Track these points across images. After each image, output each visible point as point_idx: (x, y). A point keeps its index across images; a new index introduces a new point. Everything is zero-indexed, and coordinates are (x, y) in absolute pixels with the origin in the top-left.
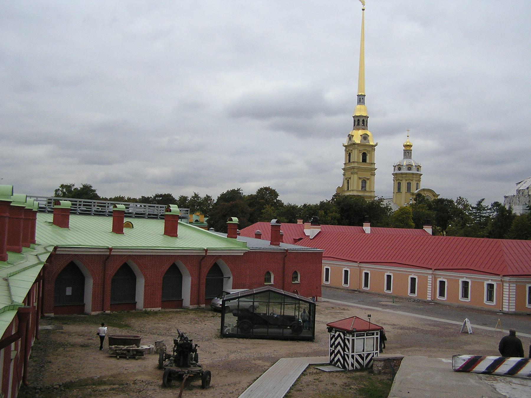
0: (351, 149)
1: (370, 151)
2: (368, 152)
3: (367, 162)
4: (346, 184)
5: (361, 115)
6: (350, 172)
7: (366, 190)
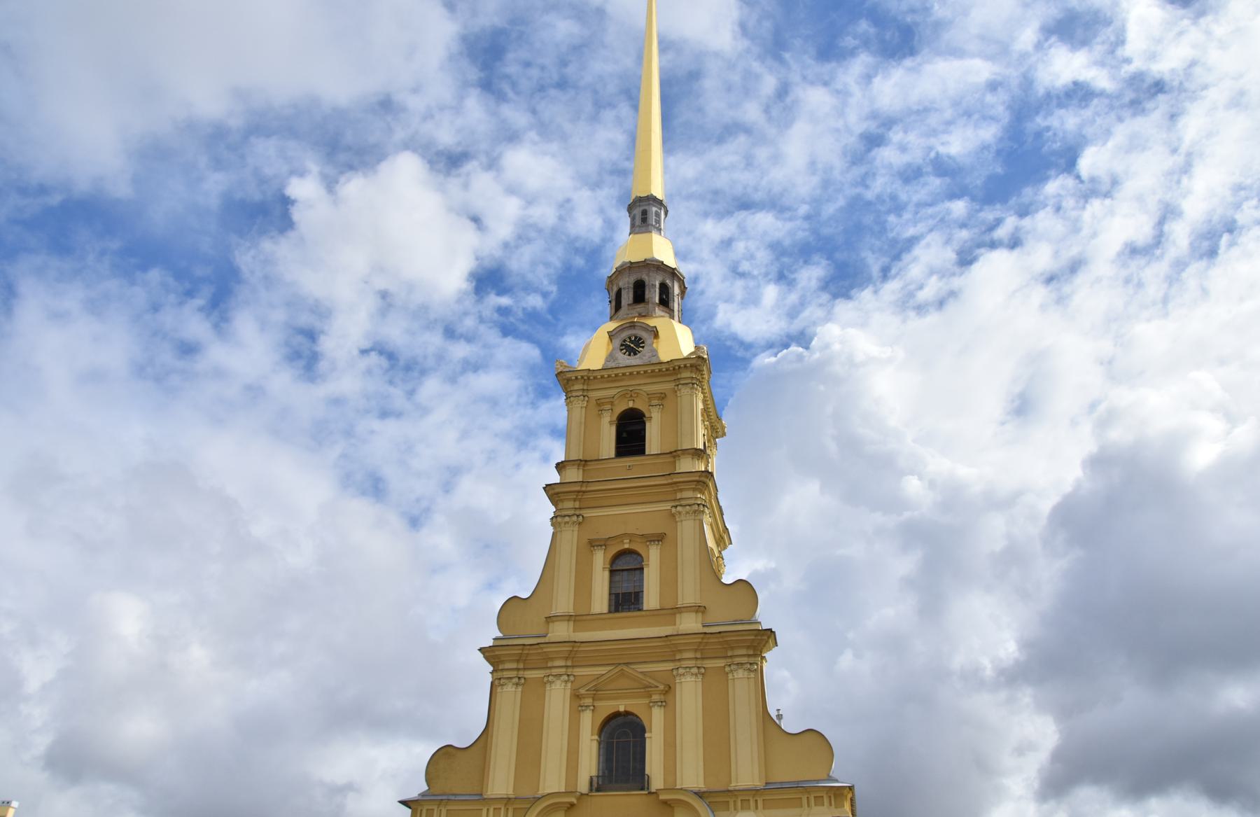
1: (662, 396)
2: (655, 402)
7: (640, 610)
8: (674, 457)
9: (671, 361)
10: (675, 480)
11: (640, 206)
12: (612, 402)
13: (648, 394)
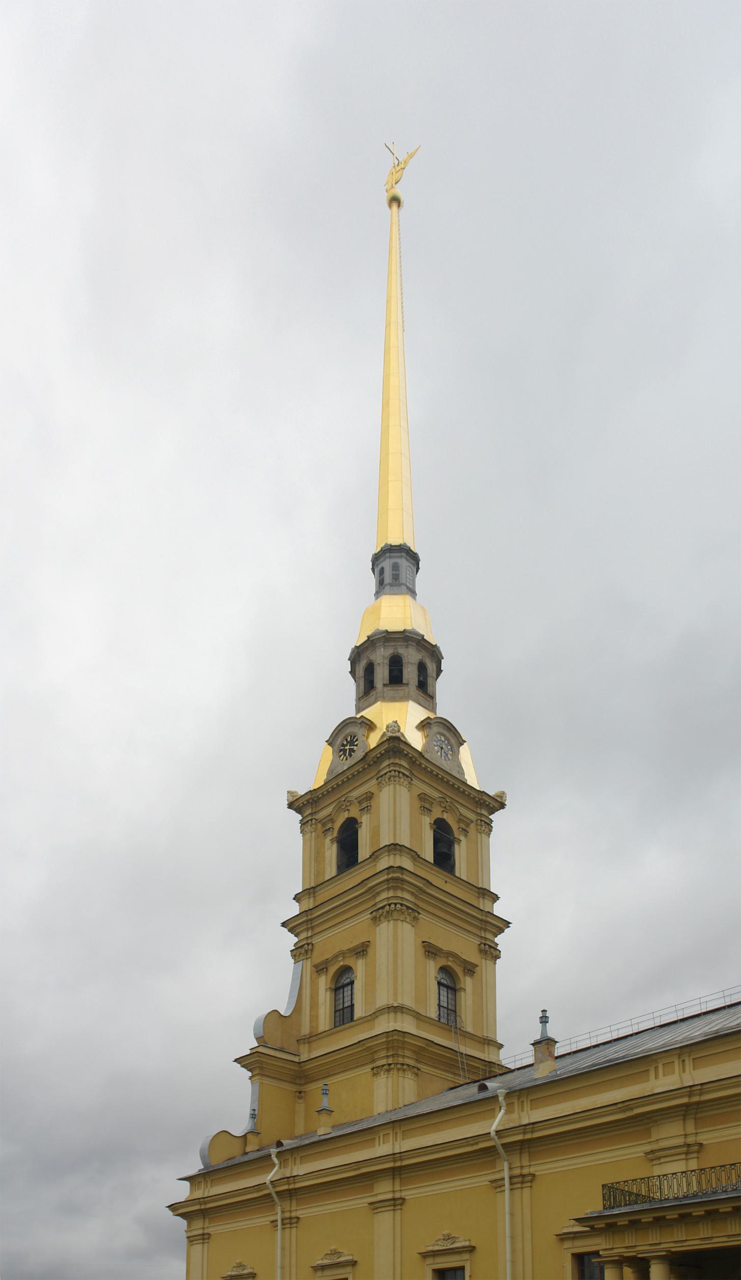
0: (371, 786)
1: (468, 823)
2: (462, 826)
3: (457, 874)
4: (325, 998)
5: (414, 632)
6: (367, 916)
8: (479, 893)
9: (483, 792)
10: (489, 920)
11: (407, 560)
12: (433, 803)
13: (461, 814)
